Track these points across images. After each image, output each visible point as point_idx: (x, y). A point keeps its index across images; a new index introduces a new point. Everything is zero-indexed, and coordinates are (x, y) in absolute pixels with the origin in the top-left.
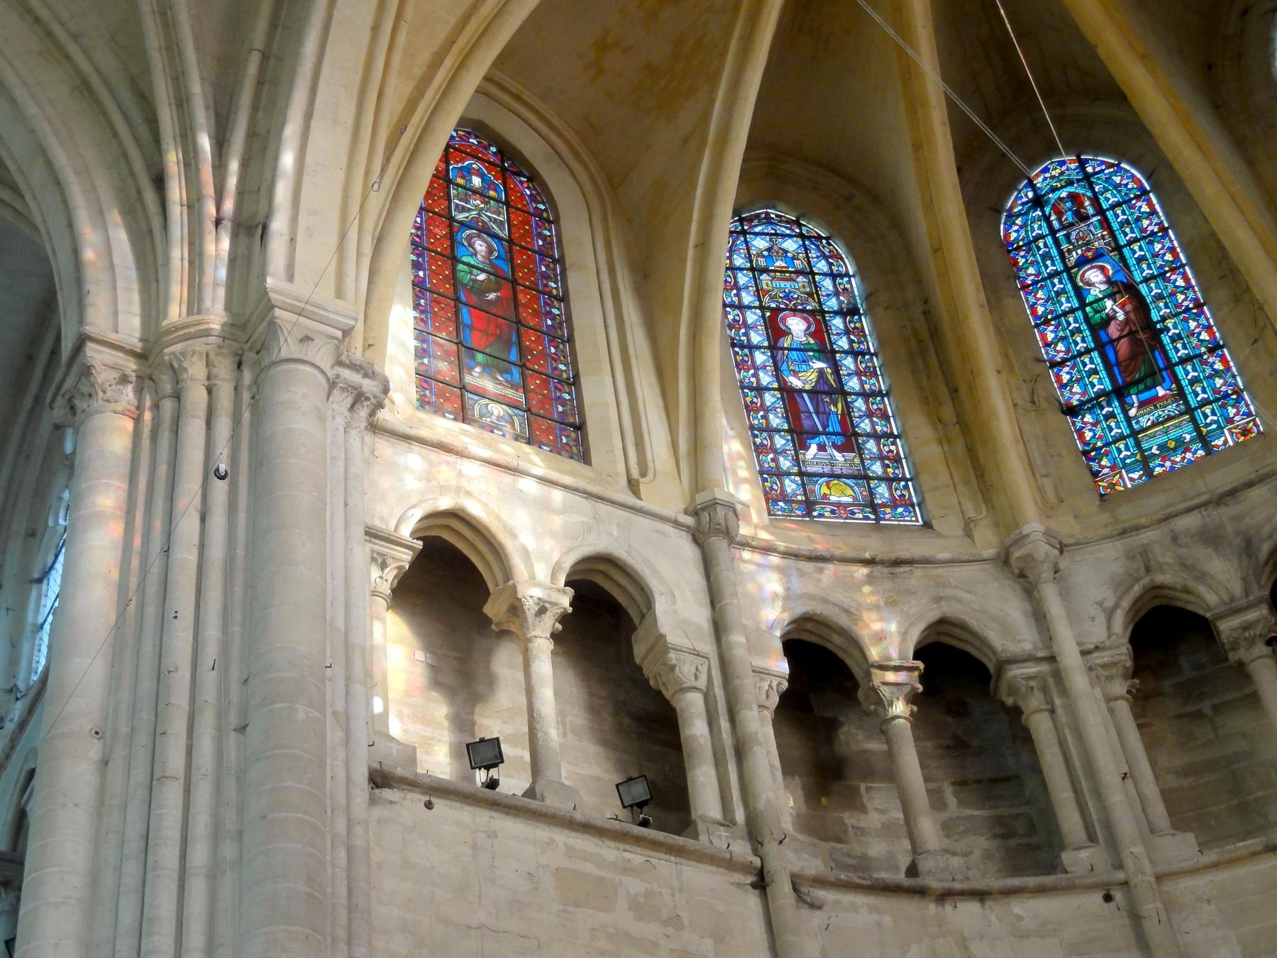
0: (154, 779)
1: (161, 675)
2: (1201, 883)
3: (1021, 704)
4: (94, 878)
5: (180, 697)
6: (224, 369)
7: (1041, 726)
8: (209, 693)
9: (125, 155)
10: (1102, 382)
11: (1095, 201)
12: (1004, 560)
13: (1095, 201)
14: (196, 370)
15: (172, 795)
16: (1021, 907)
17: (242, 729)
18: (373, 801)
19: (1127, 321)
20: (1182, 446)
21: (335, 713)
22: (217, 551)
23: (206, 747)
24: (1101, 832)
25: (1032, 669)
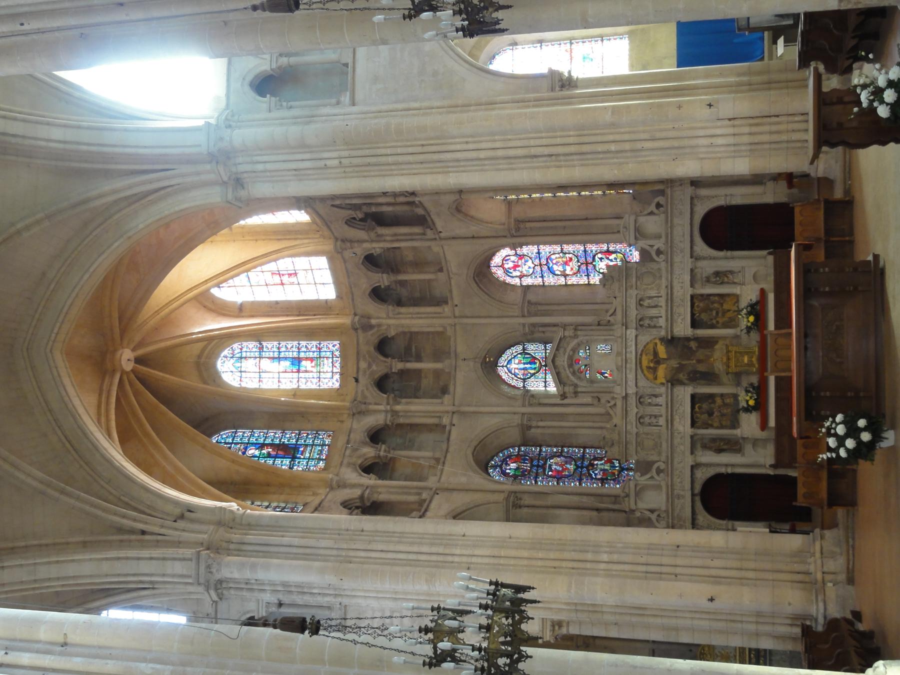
2: (443, 479)
3: (375, 499)
7: (382, 497)
9: (121, 541)
10: (287, 461)
11: (225, 443)
12: (332, 488)
13: (225, 443)
16: (433, 505)
19: (273, 450)
20: (321, 451)
24: (419, 491)
25: (367, 492)
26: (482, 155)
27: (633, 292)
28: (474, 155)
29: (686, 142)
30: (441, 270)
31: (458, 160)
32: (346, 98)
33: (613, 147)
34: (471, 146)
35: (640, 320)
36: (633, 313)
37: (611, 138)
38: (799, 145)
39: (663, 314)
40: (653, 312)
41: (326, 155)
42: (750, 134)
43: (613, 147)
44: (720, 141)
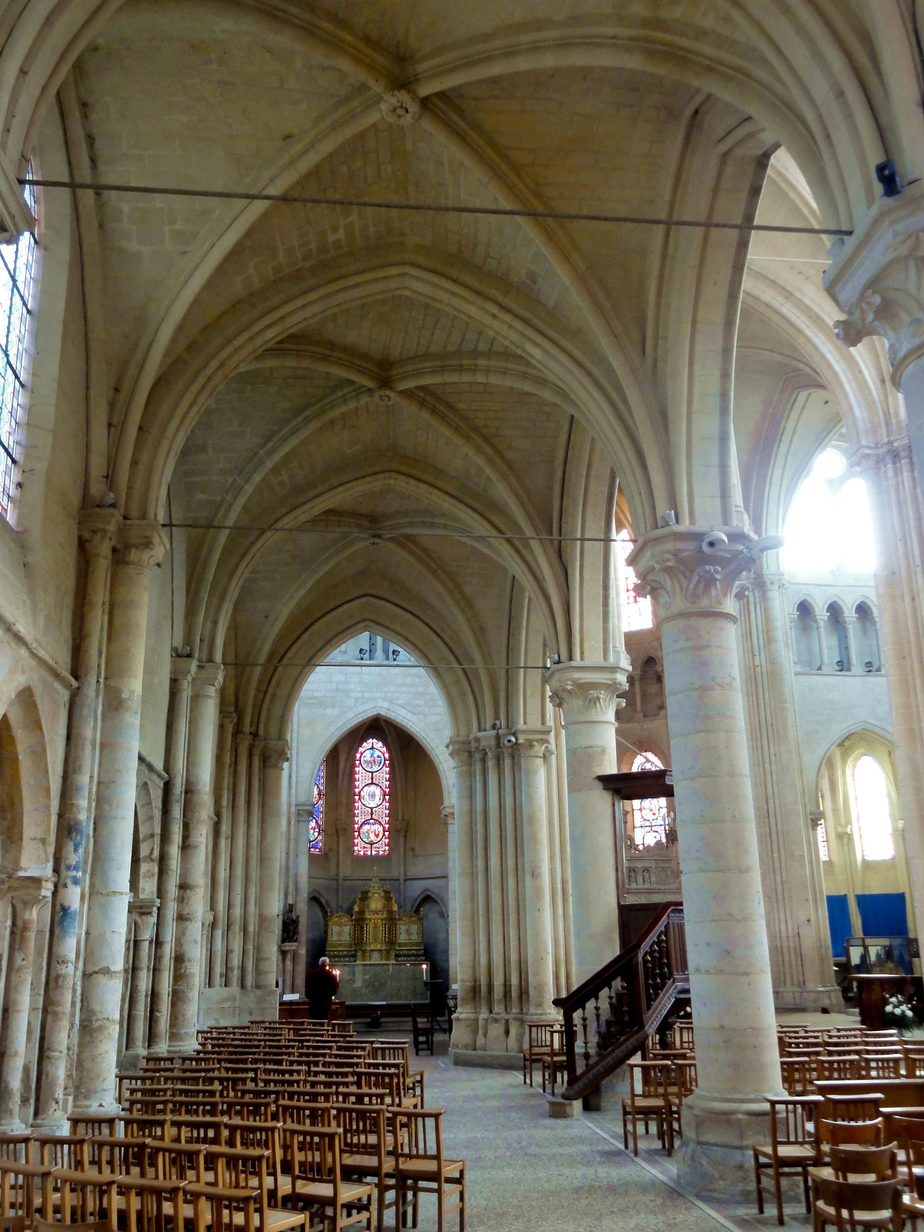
26: (767, 766)
27: (653, 865)
28: (767, 760)
29: (781, 904)
30: (645, 716)
31: (762, 749)
32: (798, 669)
33: (776, 855)
34: (773, 758)
35: (634, 871)
36: (639, 865)
37: (782, 854)
38: (782, 979)
39: (641, 886)
40: (640, 880)
41: (763, 656)
42: (789, 948)
43: (776, 855)
44: (783, 927)
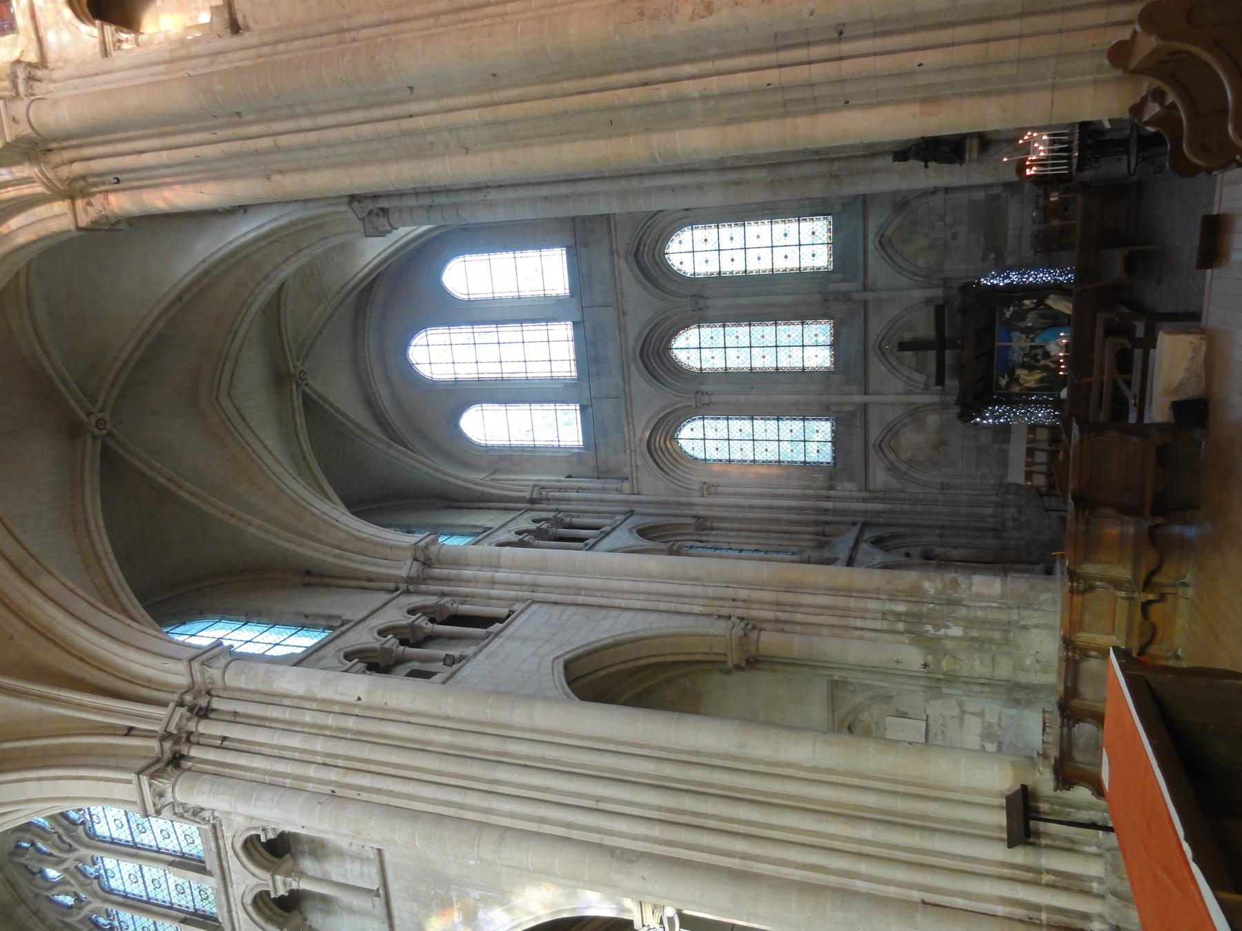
0: (278, 149)
1: (229, 157)
4: (334, 166)
5: (236, 146)
6: (56, 158)
8: (229, 133)
14: (65, 172)
15: (284, 141)
17: (239, 114)
18: (248, 29)
21: (212, 63)
22: (156, 143)
23: (254, 129)
